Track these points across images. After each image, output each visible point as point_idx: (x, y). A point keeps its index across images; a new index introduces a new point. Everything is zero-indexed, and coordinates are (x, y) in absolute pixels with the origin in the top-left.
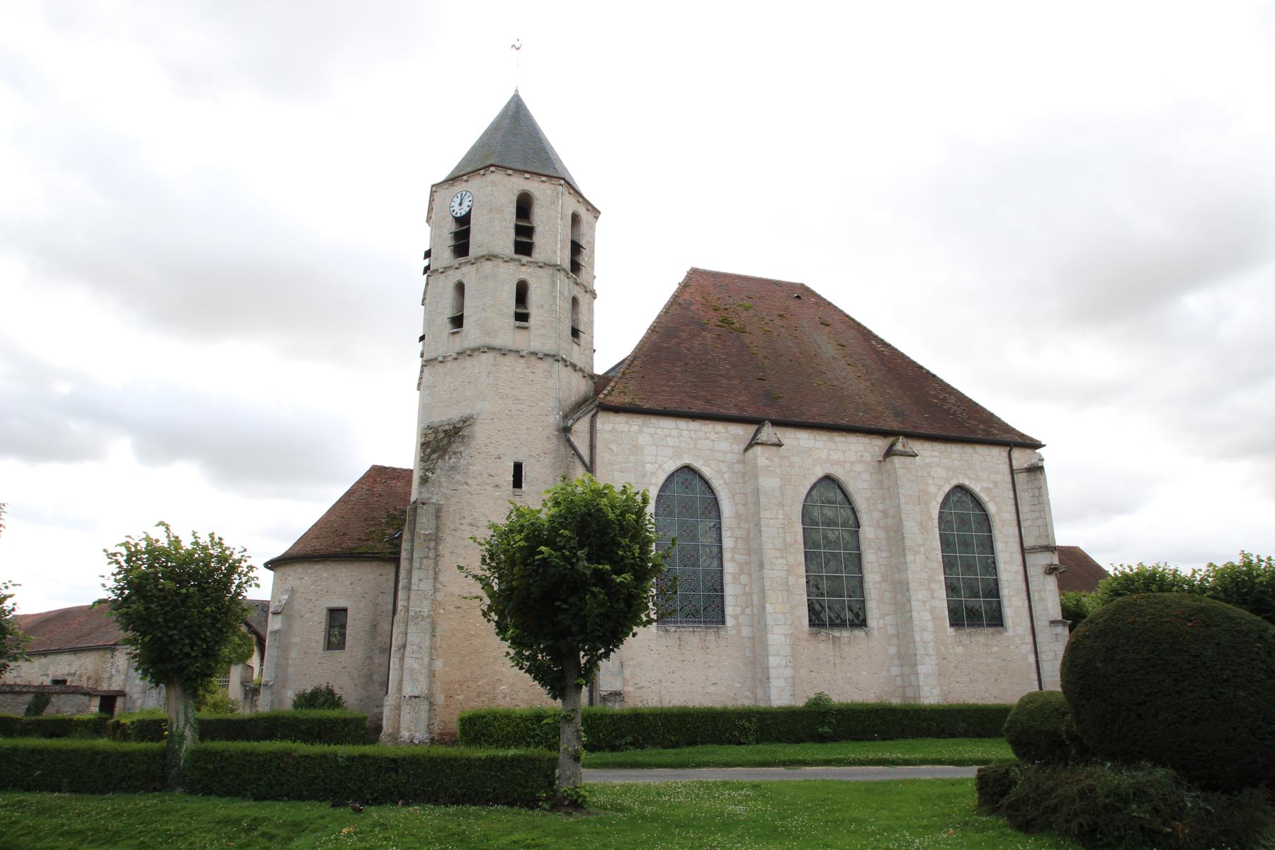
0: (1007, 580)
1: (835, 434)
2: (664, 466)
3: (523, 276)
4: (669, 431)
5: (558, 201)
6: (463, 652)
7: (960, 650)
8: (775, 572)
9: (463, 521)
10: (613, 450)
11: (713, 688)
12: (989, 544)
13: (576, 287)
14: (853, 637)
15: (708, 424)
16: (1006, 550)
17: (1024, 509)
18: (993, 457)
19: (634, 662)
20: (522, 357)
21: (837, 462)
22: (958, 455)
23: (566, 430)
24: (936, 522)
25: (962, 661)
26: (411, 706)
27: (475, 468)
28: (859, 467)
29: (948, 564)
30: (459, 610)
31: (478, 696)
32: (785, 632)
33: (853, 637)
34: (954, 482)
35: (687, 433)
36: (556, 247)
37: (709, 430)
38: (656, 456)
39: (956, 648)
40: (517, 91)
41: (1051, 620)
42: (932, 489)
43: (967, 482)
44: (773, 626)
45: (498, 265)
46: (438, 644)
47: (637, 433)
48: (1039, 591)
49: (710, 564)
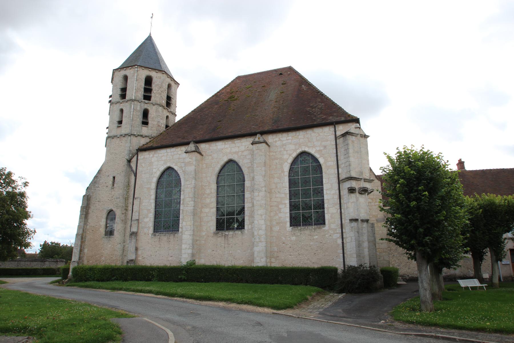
0: (327, 199)
1: (235, 140)
2: (160, 169)
3: (121, 107)
4: (163, 154)
5: (135, 74)
6: (93, 246)
7: (294, 238)
8: (188, 207)
9: (97, 200)
10: (143, 166)
11: (171, 258)
12: (320, 182)
13: (146, 105)
14: (234, 235)
15: (179, 148)
16: (328, 183)
17: (341, 157)
18: (325, 132)
19: (143, 248)
20: (118, 137)
21: (237, 153)
22: (303, 136)
23: (129, 161)
24: (287, 174)
25: (294, 244)
26: (73, 264)
27: (101, 181)
28: (246, 153)
29: (292, 195)
30: (93, 231)
31: (96, 261)
32: (190, 234)
33: (234, 235)
34: (299, 151)
35: (170, 153)
36: (133, 92)
37: (179, 150)
38: (157, 165)
39: (291, 237)
40: (150, 34)
41: (351, 218)
42: (286, 157)
43: (307, 149)
44: (185, 231)
45: (114, 106)
46: (86, 244)
47: (152, 157)
48: (346, 203)
49: (176, 206)
